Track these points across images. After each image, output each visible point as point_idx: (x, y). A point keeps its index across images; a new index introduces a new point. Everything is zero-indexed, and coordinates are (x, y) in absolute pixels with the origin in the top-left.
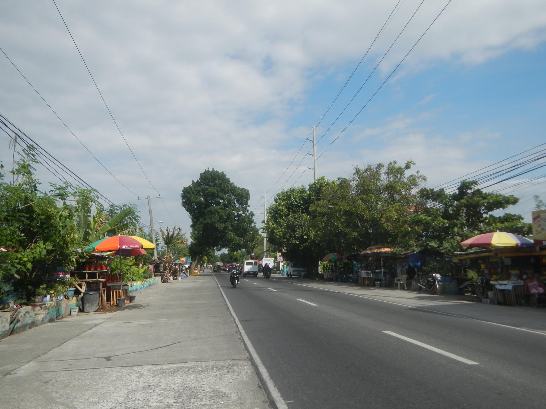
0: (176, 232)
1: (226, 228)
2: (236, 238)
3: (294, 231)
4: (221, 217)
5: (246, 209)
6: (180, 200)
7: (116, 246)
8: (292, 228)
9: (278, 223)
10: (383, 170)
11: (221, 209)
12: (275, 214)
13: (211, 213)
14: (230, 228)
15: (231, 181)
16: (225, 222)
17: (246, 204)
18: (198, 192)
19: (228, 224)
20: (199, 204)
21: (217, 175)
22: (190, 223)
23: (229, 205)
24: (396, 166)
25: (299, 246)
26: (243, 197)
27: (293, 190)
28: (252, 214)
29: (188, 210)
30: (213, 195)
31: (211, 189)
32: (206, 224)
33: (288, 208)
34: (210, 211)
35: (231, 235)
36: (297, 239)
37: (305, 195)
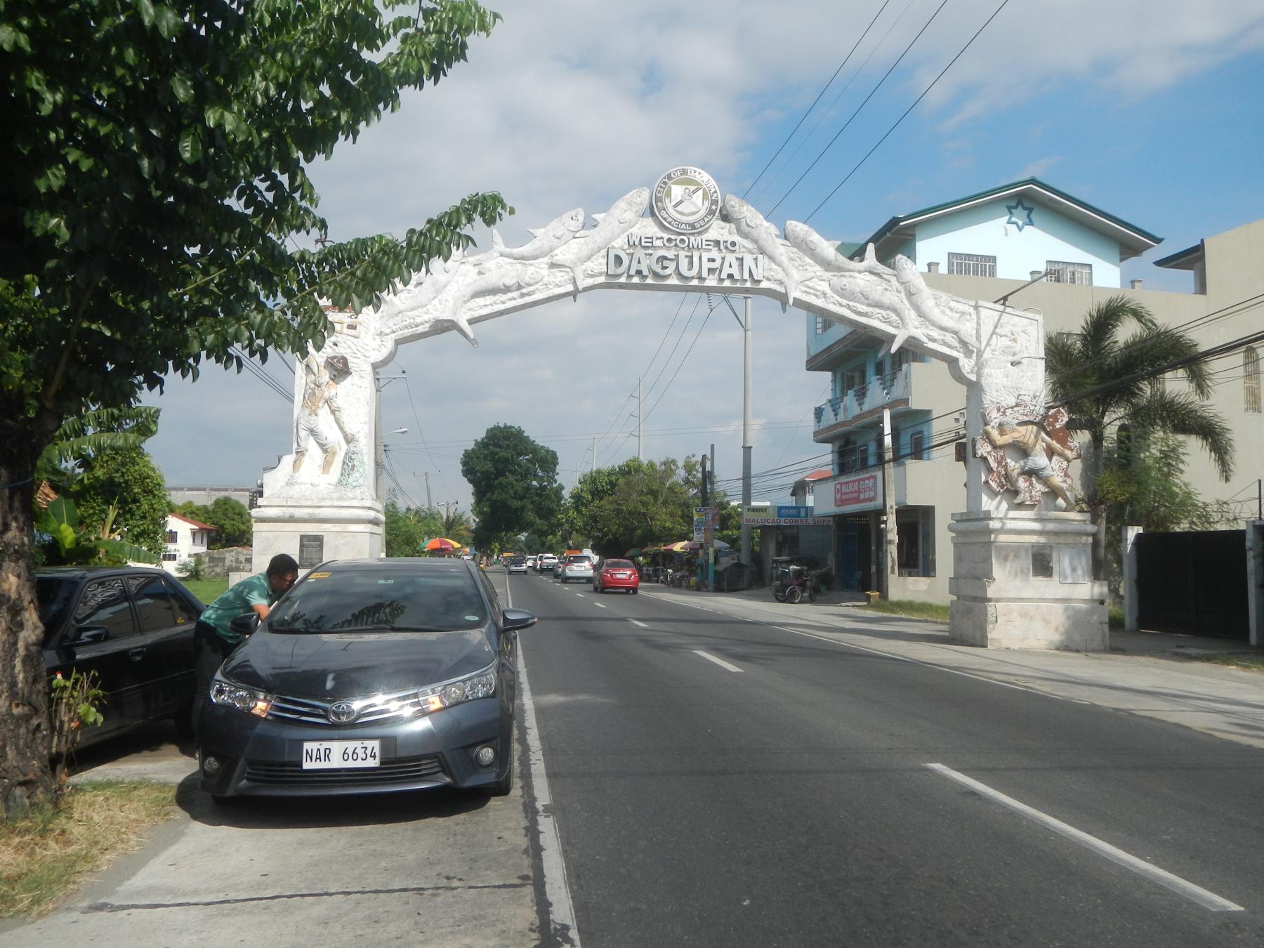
0: (452, 510)
1: (523, 508)
2: (538, 521)
3: (596, 522)
4: (516, 493)
5: (553, 478)
6: (460, 467)
7: (437, 545)
8: (594, 518)
9: (579, 512)
10: (681, 463)
11: (517, 480)
12: (577, 497)
13: (503, 487)
14: (530, 507)
15: (532, 439)
16: (521, 498)
17: (554, 471)
18: (485, 457)
19: (527, 502)
20: (486, 475)
21: (512, 433)
22: (472, 500)
23: (526, 474)
24: (693, 460)
25: (602, 539)
26: (548, 461)
27: (598, 472)
28: (561, 488)
29: (470, 481)
30: (506, 460)
31: (503, 453)
32: (496, 501)
33: (593, 494)
34: (501, 484)
35: (531, 516)
36: (600, 530)
37: (613, 478)
